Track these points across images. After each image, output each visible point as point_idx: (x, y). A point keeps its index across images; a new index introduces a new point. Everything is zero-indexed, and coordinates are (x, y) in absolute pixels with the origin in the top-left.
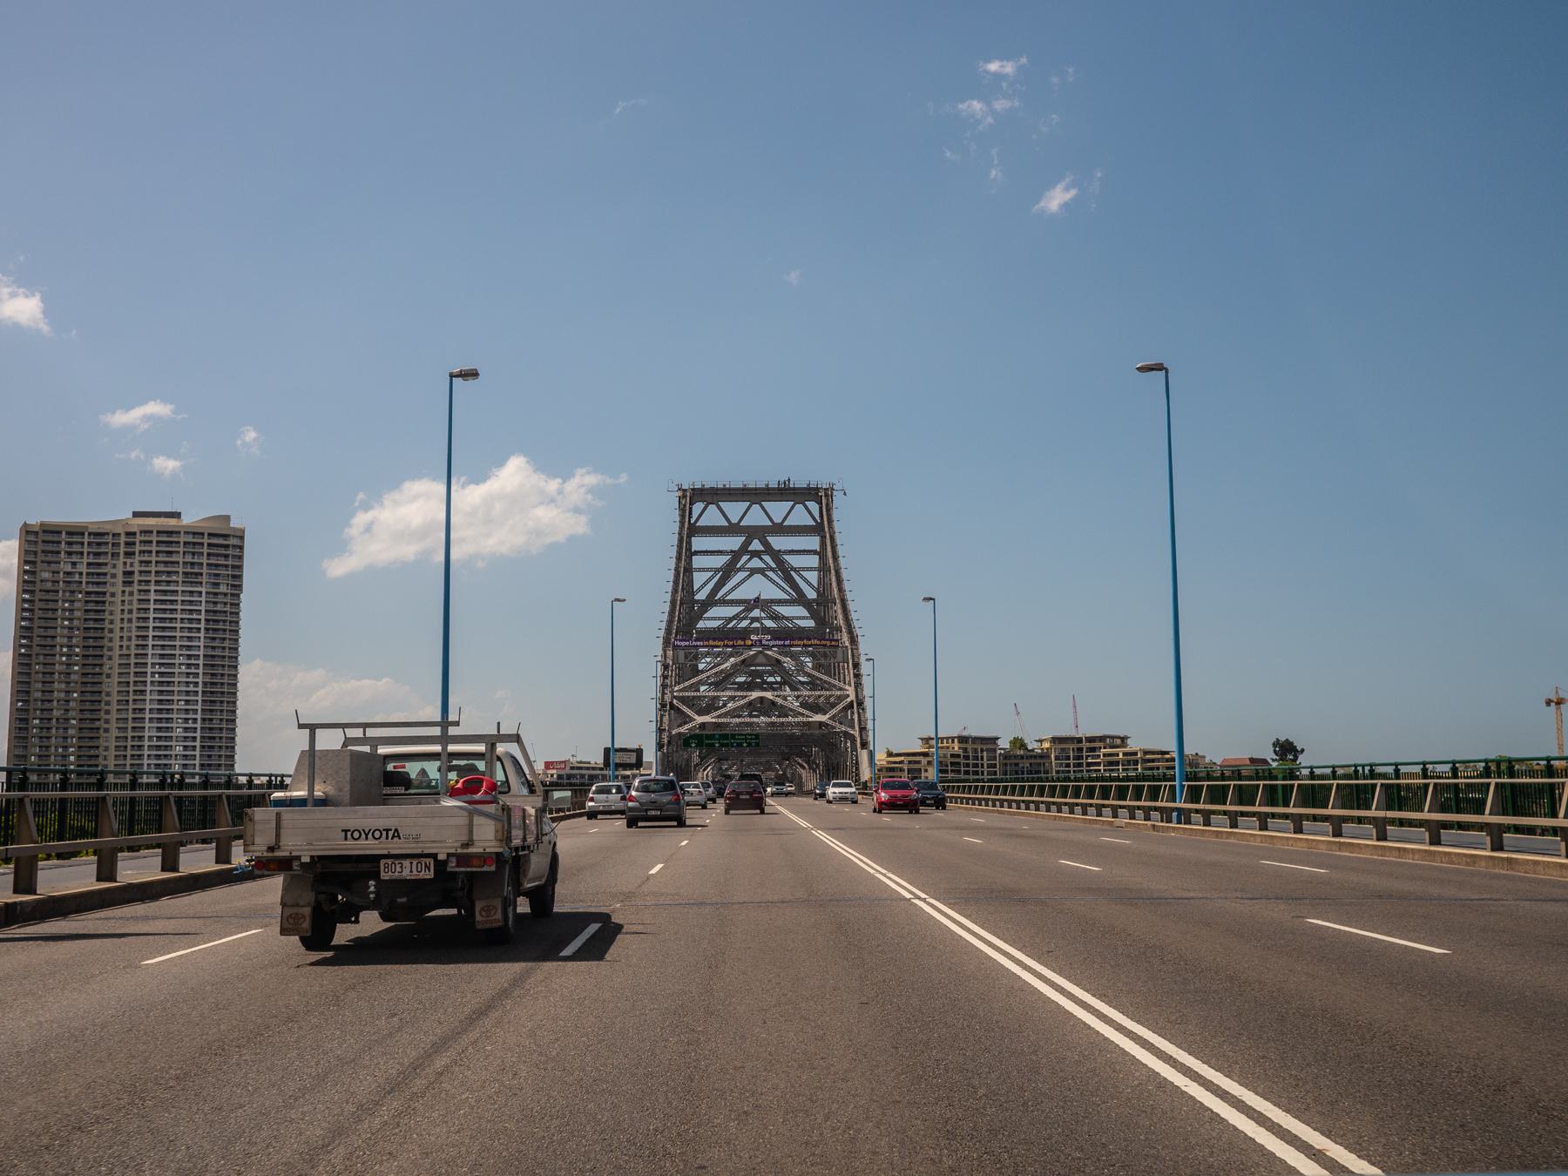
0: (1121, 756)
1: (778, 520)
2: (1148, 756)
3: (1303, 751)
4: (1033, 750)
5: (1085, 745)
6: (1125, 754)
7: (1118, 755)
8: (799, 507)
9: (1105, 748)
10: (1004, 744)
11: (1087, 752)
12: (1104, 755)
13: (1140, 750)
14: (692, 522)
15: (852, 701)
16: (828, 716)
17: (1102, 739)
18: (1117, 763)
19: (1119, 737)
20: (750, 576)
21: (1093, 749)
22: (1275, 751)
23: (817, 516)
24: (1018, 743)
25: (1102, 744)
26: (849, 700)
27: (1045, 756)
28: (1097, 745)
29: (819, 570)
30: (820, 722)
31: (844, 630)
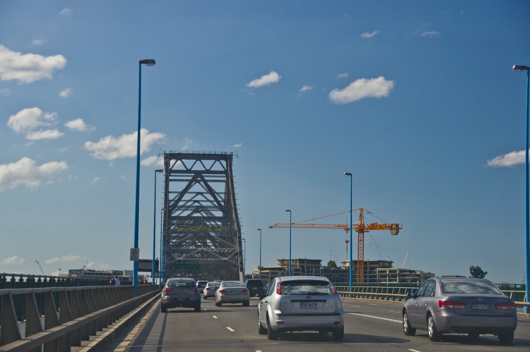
0: (388, 272)
1: (208, 168)
2: (402, 274)
3: (486, 273)
4: (340, 268)
5: (368, 266)
6: (390, 271)
7: (386, 272)
8: (217, 162)
9: (379, 268)
10: (324, 264)
11: (369, 270)
12: (379, 272)
13: (398, 269)
14: (170, 167)
15: (238, 252)
16: (228, 258)
17: (378, 262)
18: (386, 276)
19: (387, 262)
20: (196, 195)
21: (373, 268)
22: (471, 272)
23: (225, 166)
24: (332, 264)
25: (378, 266)
26: (236, 252)
27: (346, 271)
28: (375, 266)
29: (225, 193)
30: (225, 261)
31: (235, 222)
